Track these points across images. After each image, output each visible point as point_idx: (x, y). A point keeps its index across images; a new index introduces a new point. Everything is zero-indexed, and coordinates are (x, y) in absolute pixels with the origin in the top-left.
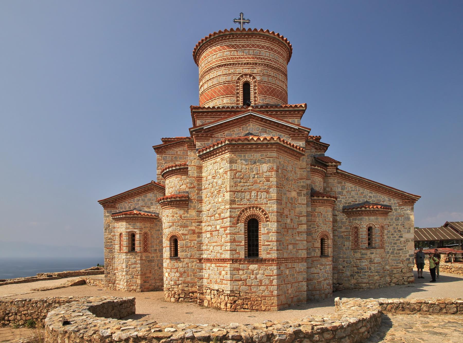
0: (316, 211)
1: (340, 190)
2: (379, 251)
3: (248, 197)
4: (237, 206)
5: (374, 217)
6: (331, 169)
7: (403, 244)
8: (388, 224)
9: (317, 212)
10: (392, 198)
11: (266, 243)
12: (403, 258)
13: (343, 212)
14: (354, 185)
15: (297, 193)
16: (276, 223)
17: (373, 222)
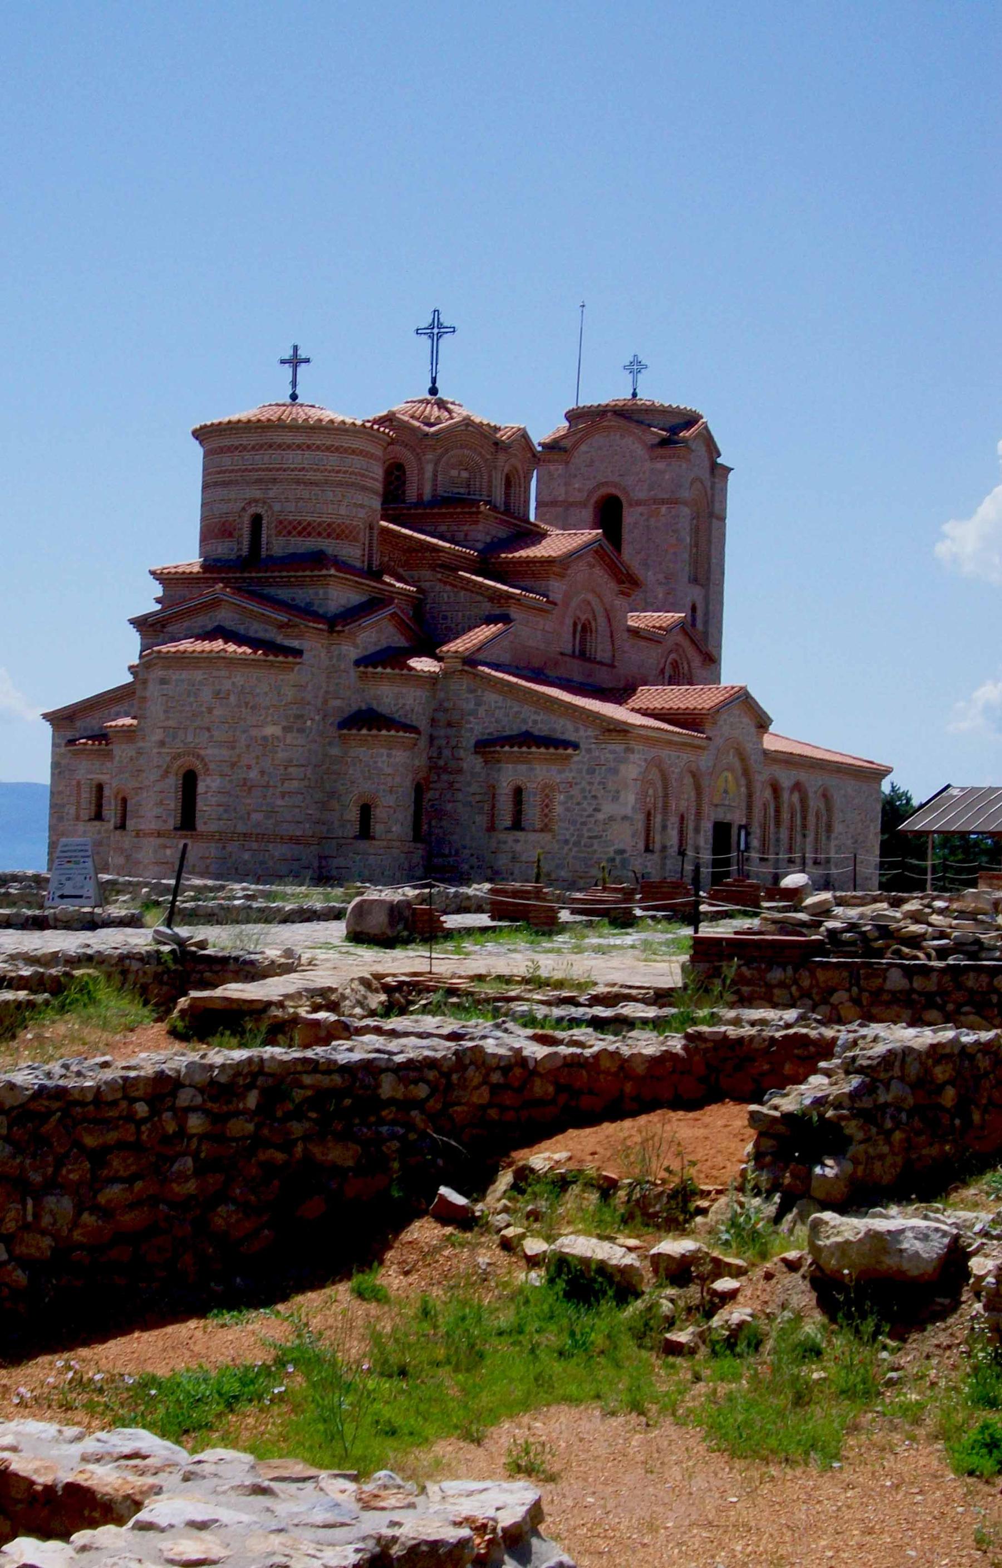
2: (532, 837)
4: (167, 750)
5: (525, 766)
11: (205, 809)
15: (284, 728)
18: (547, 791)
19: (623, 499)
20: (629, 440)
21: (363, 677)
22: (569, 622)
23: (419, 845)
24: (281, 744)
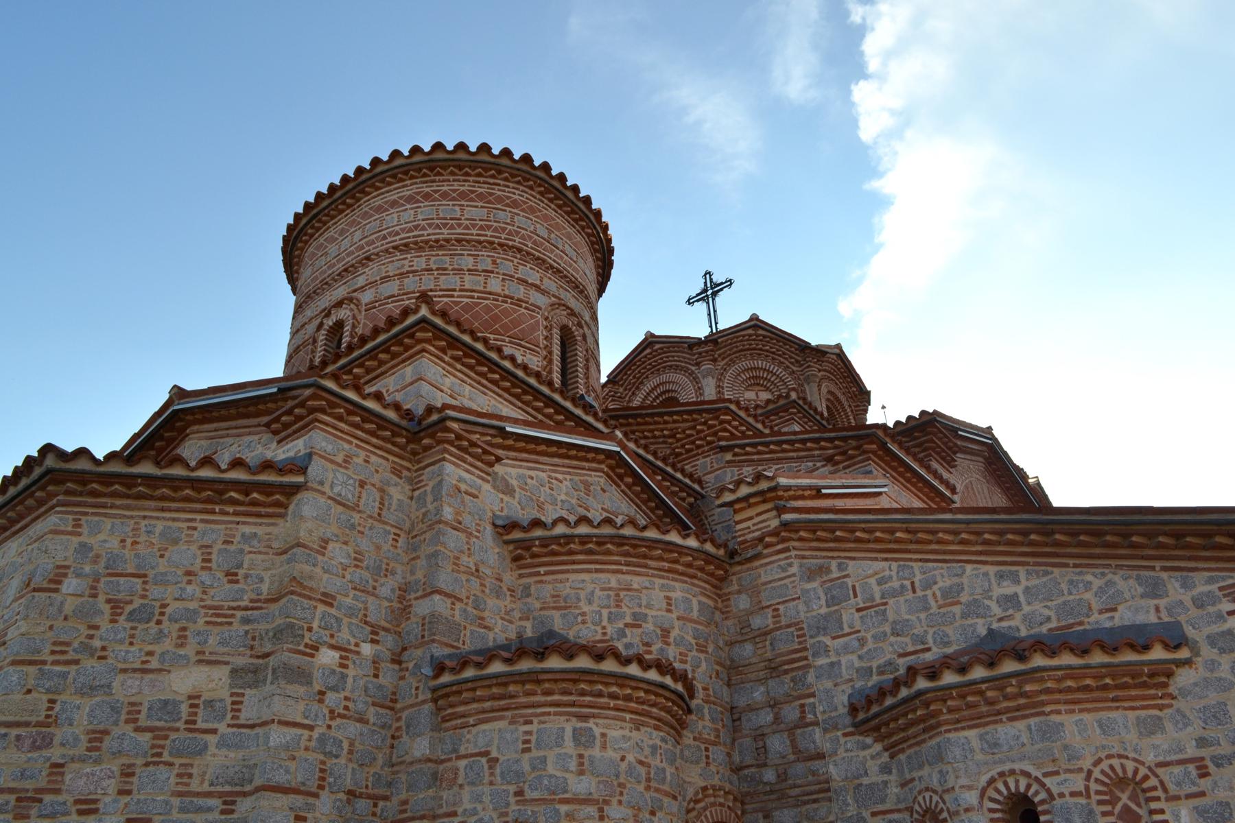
0: (462, 751)
1: (824, 611)
5: (1021, 725)
6: (751, 518)
8: (1191, 751)
9: (465, 757)
10: (1164, 569)
13: (860, 727)
14: (894, 565)
15: (234, 672)
17: (1023, 758)
18: (1124, 798)
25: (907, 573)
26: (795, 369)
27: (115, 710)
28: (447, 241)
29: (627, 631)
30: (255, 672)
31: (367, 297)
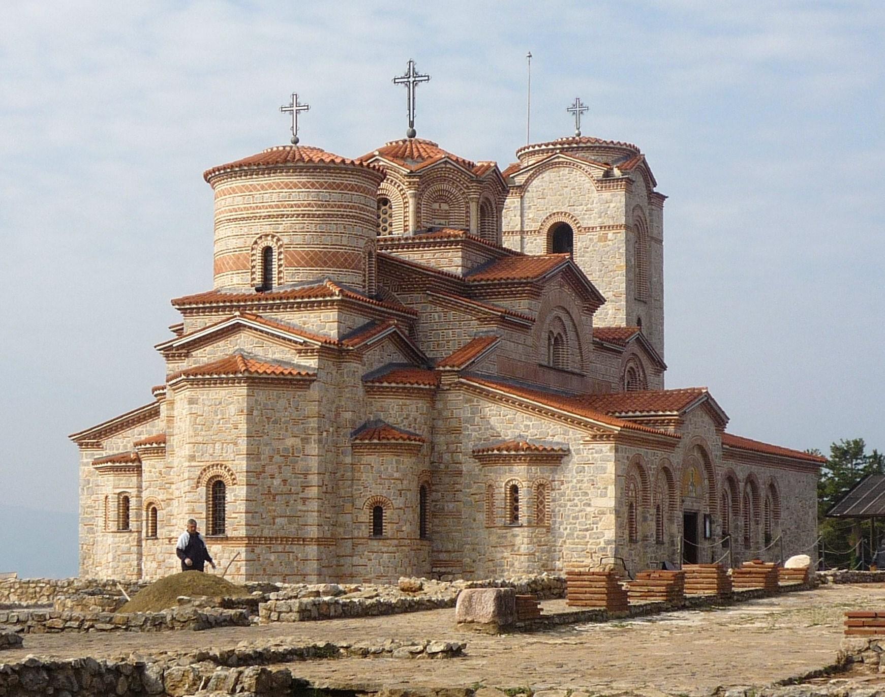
1: (469, 415)
3: (211, 452)
7: (592, 519)
12: (593, 547)
13: (475, 457)
15: (302, 440)
16: (245, 487)
18: (541, 488)
19: (573, 226)
20: (577, 173)
21: (369, 391)
22: (545, 335)
23: (425, 543)
24: (301, 455)
25: (498, 410)
26: (466, 191)
27: (273, 450)
28: (324, 214)
29: (404, 421)
30: (307, 439)
31: (285, 240)
